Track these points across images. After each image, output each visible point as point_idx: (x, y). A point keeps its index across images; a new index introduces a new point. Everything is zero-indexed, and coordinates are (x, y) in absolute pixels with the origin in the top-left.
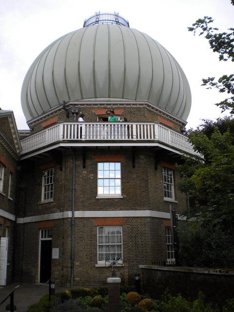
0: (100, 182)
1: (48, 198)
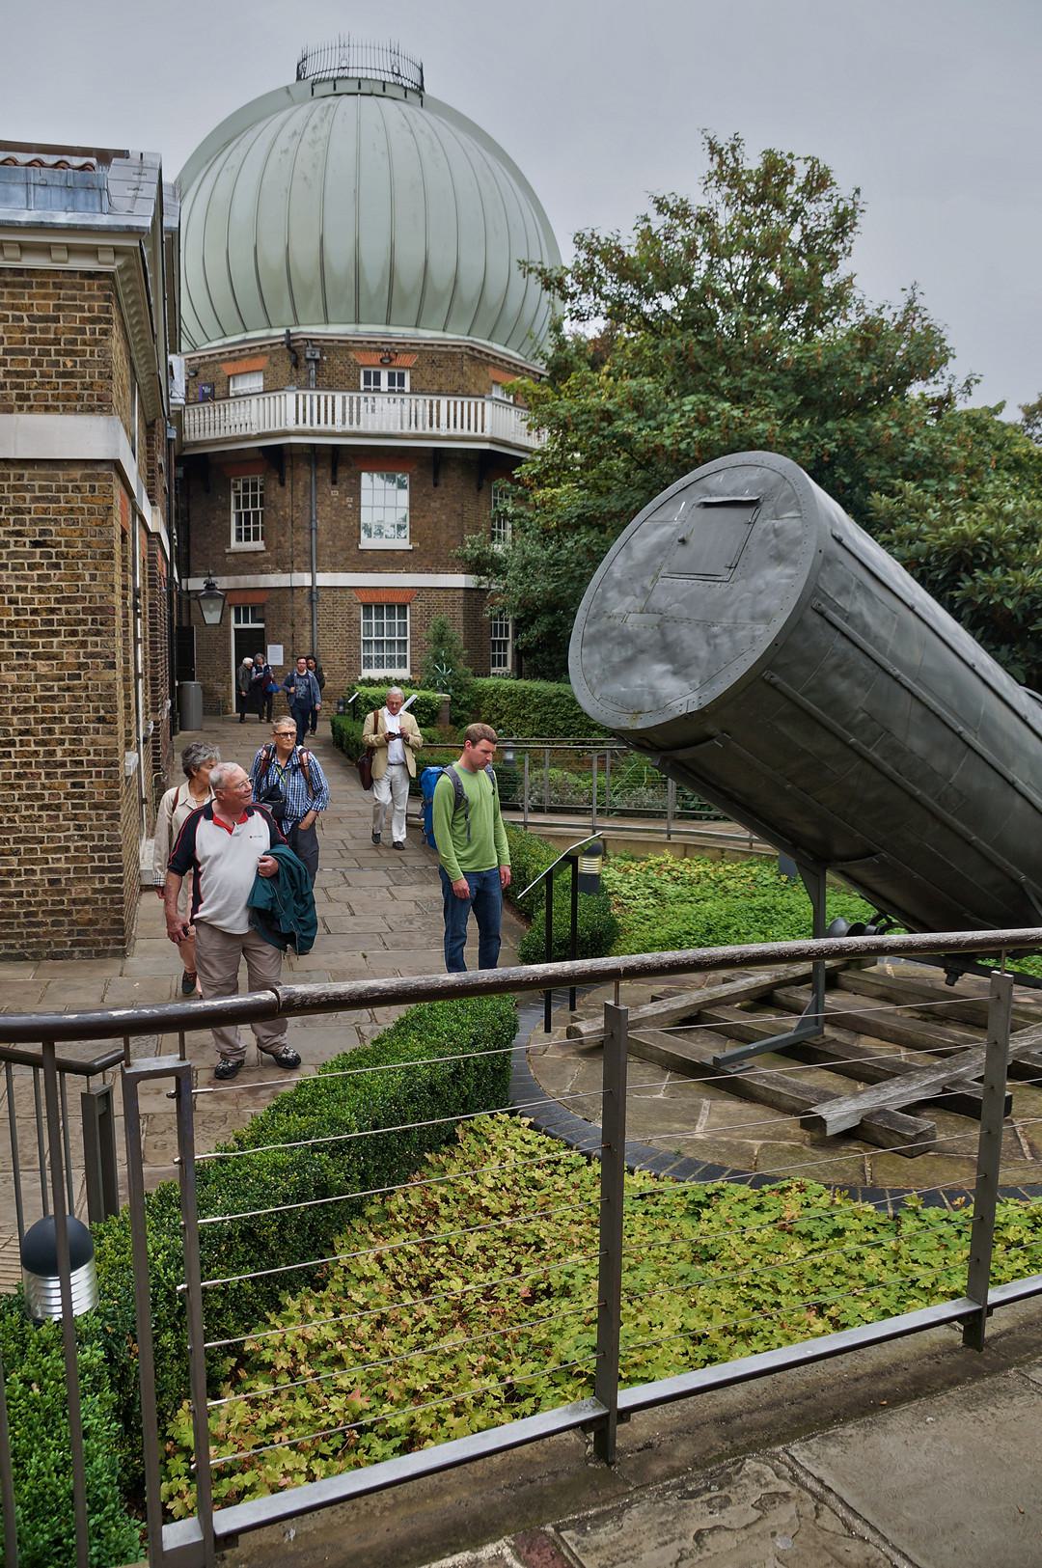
1: (248, 539)
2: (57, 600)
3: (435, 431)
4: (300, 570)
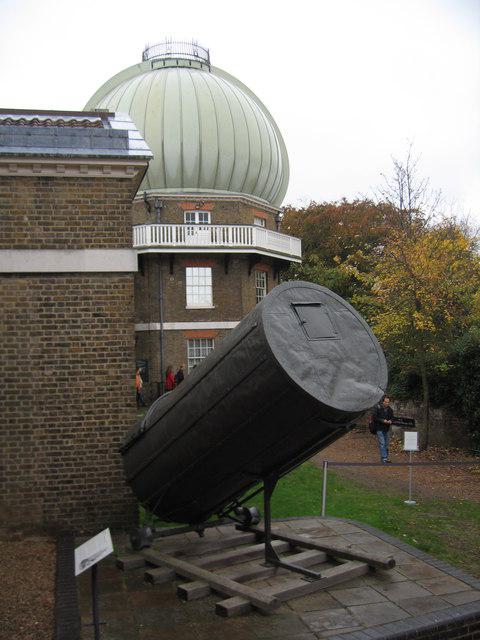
2: (106, 344)
3: (226, 244)
4: (154, 321)
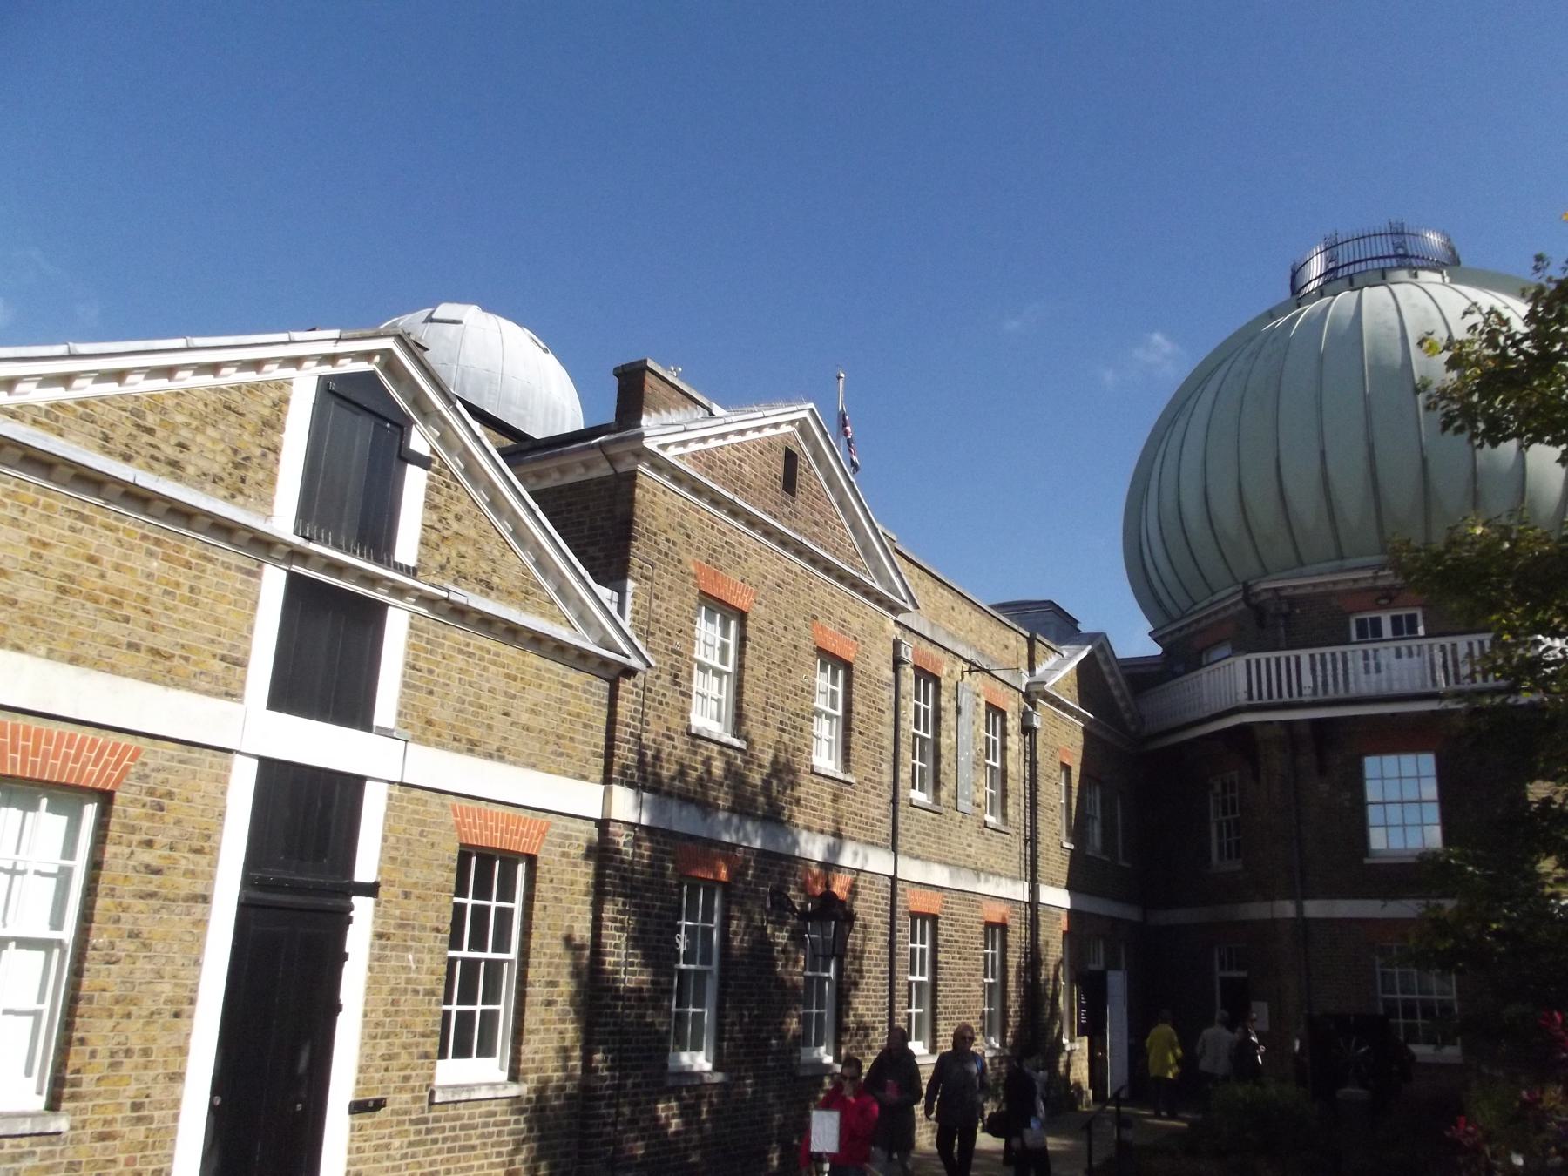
0: (1374, 814)
